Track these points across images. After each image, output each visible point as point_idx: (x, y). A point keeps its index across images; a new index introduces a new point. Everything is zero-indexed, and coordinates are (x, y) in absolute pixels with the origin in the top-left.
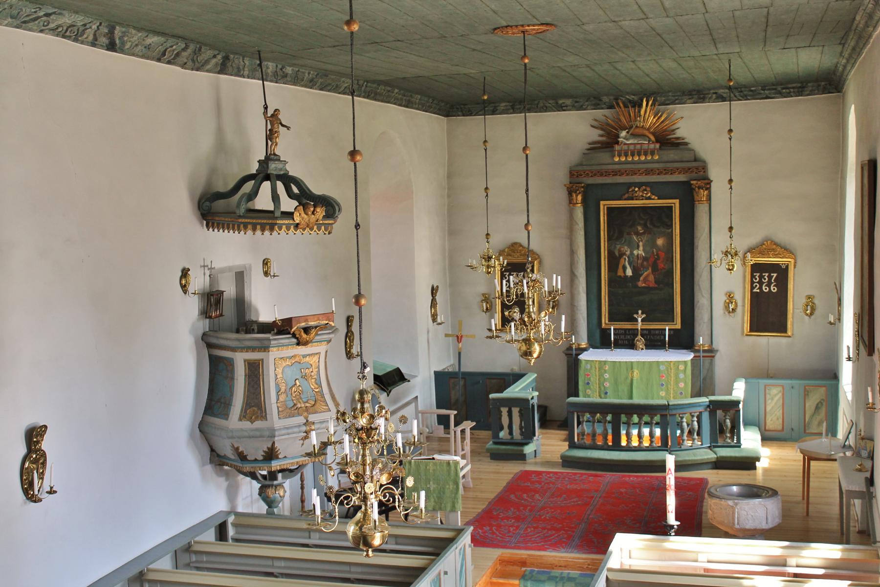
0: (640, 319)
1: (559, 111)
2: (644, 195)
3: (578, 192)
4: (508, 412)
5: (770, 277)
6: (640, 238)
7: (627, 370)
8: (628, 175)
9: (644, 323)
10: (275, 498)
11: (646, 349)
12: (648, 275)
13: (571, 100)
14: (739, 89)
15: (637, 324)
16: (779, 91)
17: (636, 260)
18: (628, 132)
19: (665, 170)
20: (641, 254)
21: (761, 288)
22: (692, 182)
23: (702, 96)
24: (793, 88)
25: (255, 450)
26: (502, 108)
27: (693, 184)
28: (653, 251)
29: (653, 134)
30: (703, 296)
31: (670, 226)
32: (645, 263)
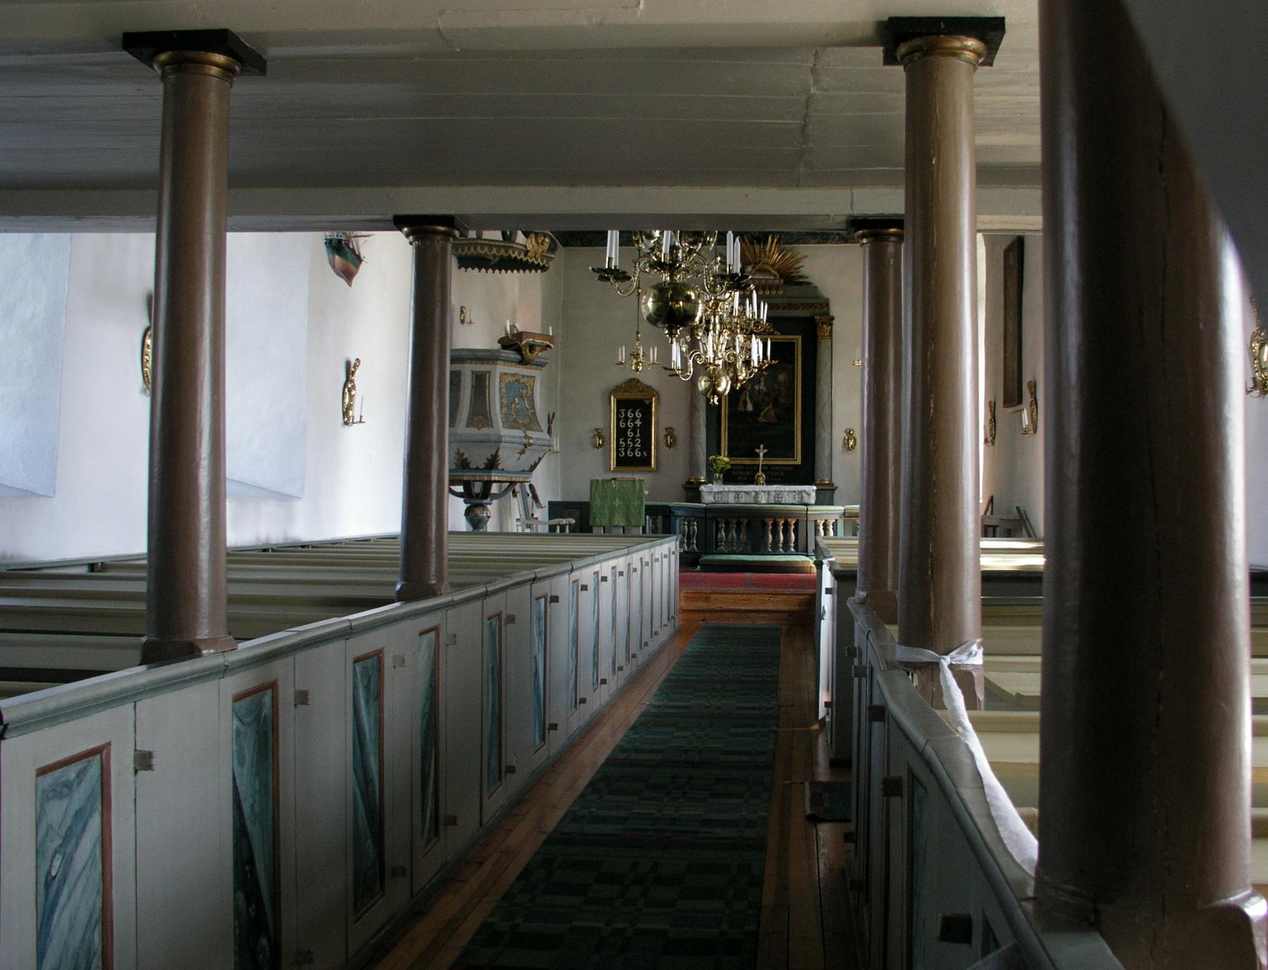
0: (761, 454)
10: (483, 517)
12: (770, 409)
18: (753, 268)
20: (763, 390)
22: (816, 317)
23: (825, 236)
25: (478, 458)
29: (778, 270)
30: (825, 430)
31: (792, 362)
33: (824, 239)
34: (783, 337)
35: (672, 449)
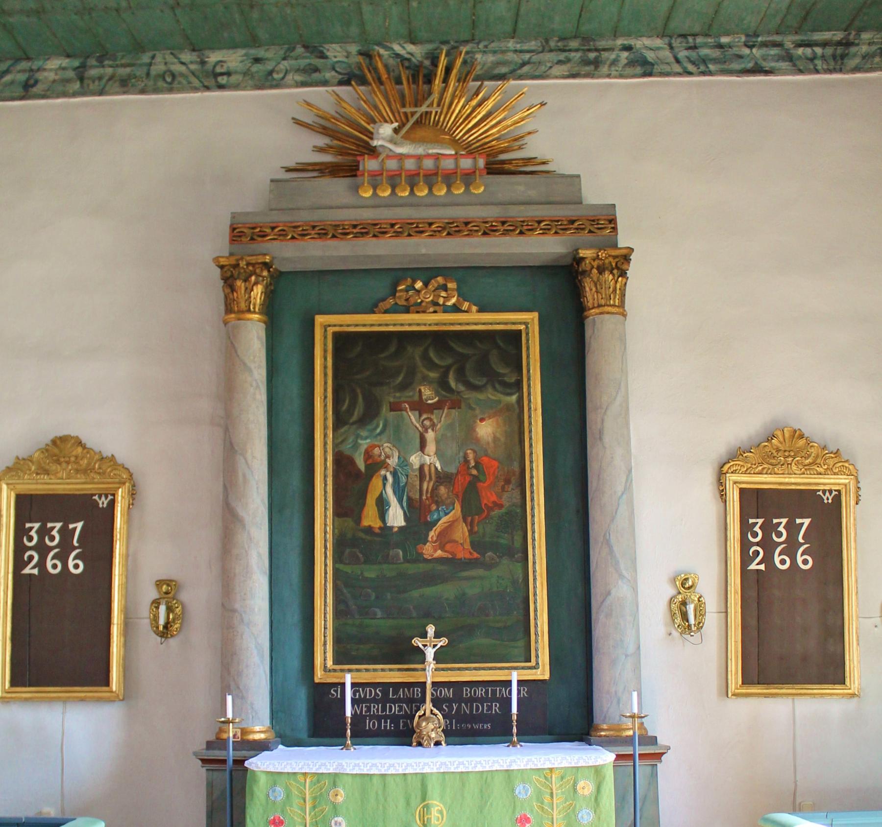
0: (430, 653)
1: (208, 88)
2: (441, 301)
3: (253, 278)
5: (793, 528)
6: (430, 419)
7: (408, 803)
8: (398, 234)
11: (448, 744)
12: (451, 525)
13: (242, 51)
14: (690, 39)
15: (424, 670)
17: (418, 483)
19: (503, 223)
21: (768, 560)
23: (592, 55)
24: (824, 44)
26: (52, 76)
27: (583, 259)
30: (621, 576)
32: (443, 490)
33: (586, 62)
35: (172, 642)
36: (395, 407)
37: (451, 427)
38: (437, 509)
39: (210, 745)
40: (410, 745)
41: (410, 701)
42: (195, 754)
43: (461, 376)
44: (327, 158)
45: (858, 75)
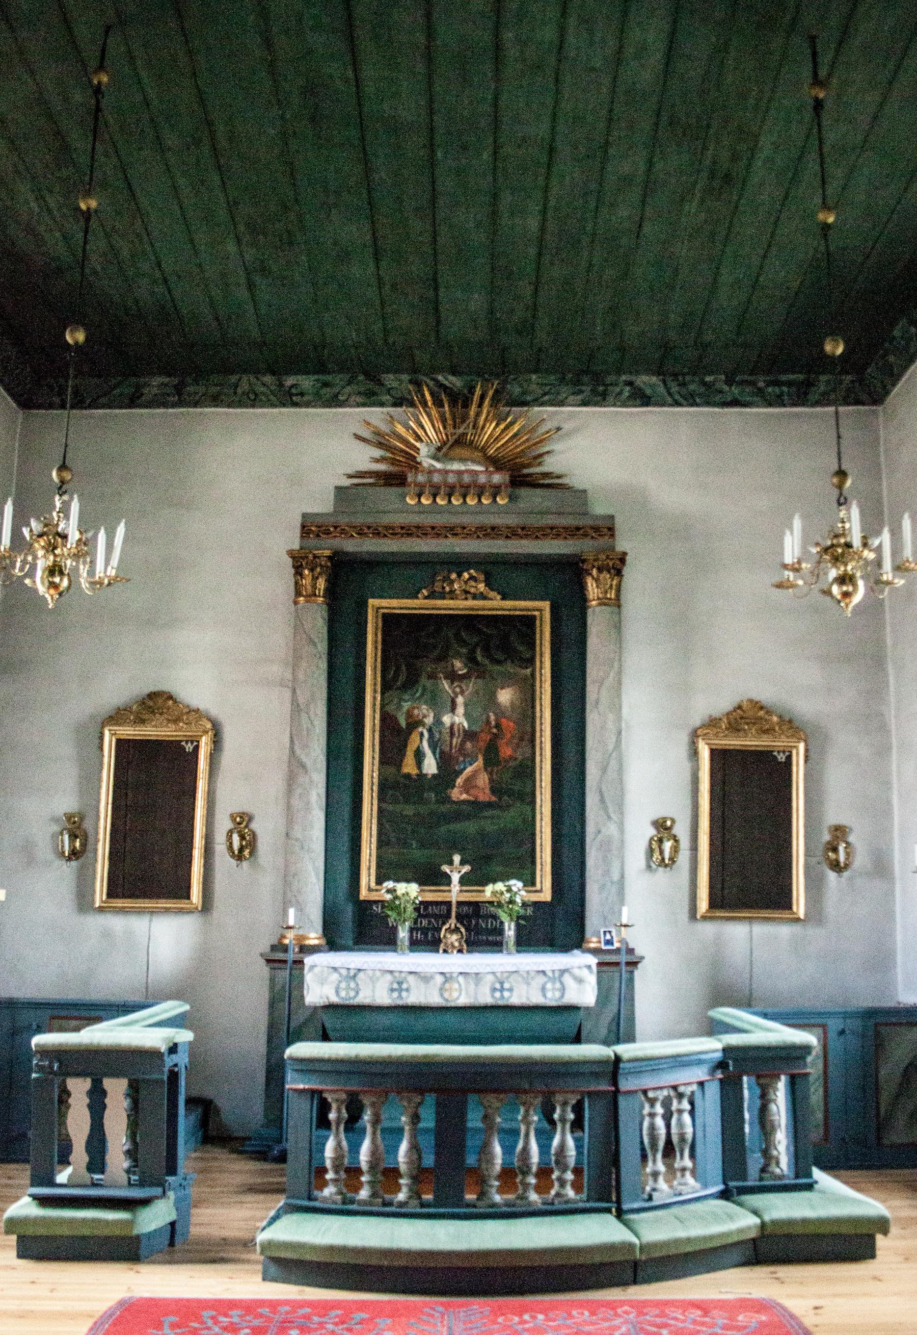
0: (455, 878)
1: (284, 405)
3: (318, 569)
4: (91, 1093)
6: (461, 687)
9: (464, 888)
11: (469, 952)
12: (474, 775)
15: (450, 891)
16: (759, 389)
17: (448, 739)
19: (523, 529)
26: (155, 391)
28: (488, 717)
30: (609, 817)
31: (530, 662)
32: (469, 745)
34: (509, 604)
35: (245, 864)
36: (432, 676)
37: (477, 692)
38: (464, 761)
39: (274, 948)
40: (438, 951)
41: (436, 916)
42: (262, 955)
43: (487, 651)
44: (382, 467)
45: (818, 409)
